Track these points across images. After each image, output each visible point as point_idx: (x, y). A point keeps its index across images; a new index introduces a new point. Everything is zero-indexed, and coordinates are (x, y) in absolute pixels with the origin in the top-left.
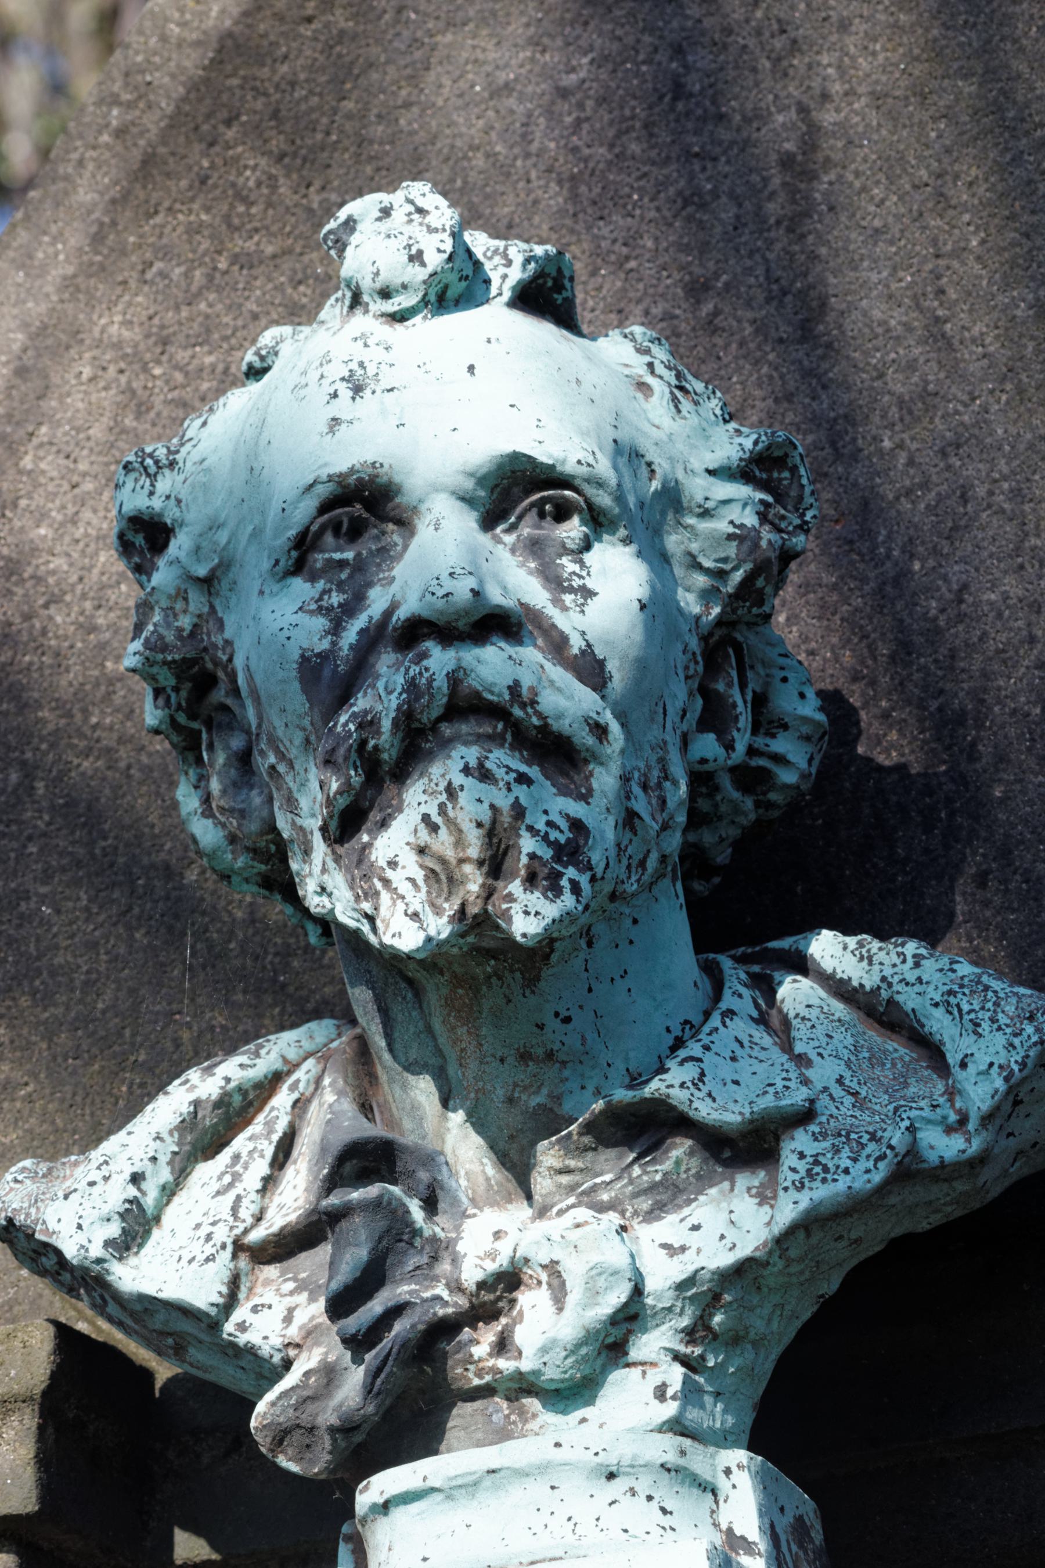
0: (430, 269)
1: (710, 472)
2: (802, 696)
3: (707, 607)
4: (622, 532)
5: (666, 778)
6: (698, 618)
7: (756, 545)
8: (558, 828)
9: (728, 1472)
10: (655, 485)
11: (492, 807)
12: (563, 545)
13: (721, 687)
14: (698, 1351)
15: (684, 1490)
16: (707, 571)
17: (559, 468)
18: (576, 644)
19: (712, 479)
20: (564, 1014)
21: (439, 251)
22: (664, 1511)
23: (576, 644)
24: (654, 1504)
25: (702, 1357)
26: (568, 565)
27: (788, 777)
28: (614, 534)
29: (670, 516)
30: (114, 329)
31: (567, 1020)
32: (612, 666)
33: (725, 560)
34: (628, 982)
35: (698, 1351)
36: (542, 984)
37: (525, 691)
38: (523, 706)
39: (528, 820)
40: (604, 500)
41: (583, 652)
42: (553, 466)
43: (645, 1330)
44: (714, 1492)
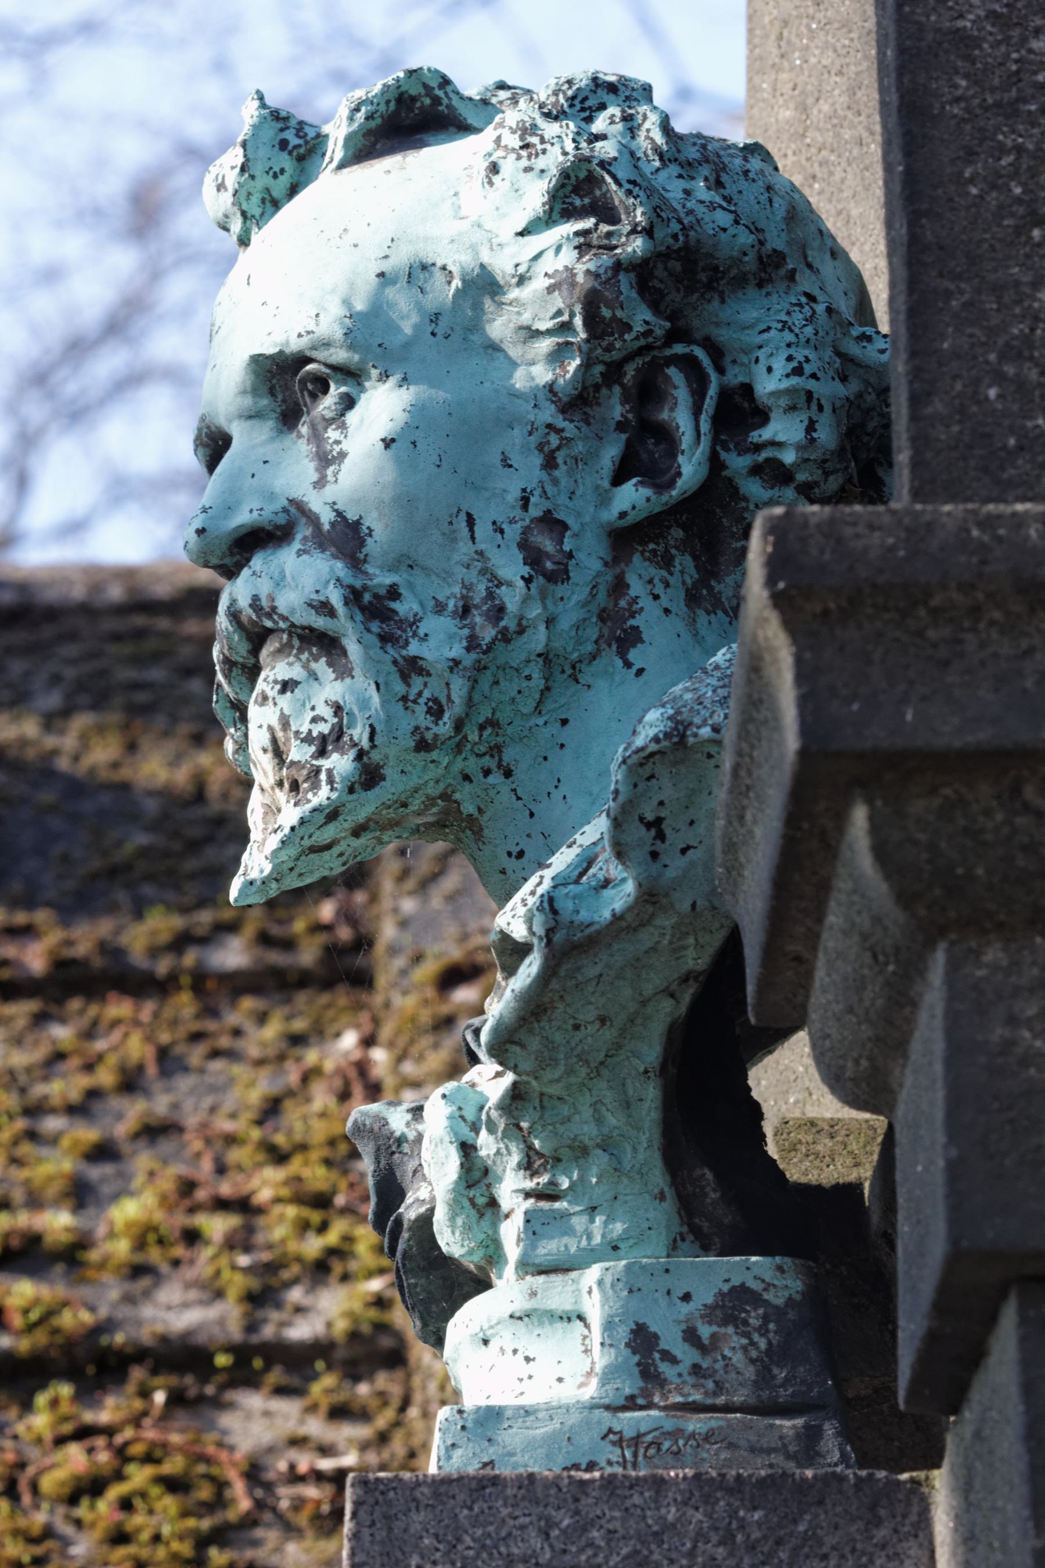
0: (231, 191)
1: (521, 234)
2: (770, 370)
3: (562, 366)
4: (374, 373)
5: (500, 585)
6: (550, 388)
7: (573, 284)
8: (323, 719)
9: (590, 1292)
10: (457, 283)
11: (271, 729)
12: (324, 419)
13: (665, 415)
14: (544, 1179)
15: (547, 1330)
16: (549, 332)
17: (287, 351)
18: (327, 517)
19: (527, 238)
20: (515, 850)
21: (233, 168)
22: (528, 1359)
23: (327, 517)
24: (520, 1356)
25: (552, 1183)
26: (332, 434)
27: (789, 457)
28: (369, 378)
29: (488, 304)
30: (780, 117)
31: (521, 854)
32: (372, 521)
33: (559, 313)
34: (563, 790)
35: (544, 1179)
36: (486, 832)
37: (265, 603)
38: (269, 616)
39: (294, 728)
40: (340, 355)
41: (333, 524)
42: (281, 352)
43: (500, 1179)
44: (581, 1318)
